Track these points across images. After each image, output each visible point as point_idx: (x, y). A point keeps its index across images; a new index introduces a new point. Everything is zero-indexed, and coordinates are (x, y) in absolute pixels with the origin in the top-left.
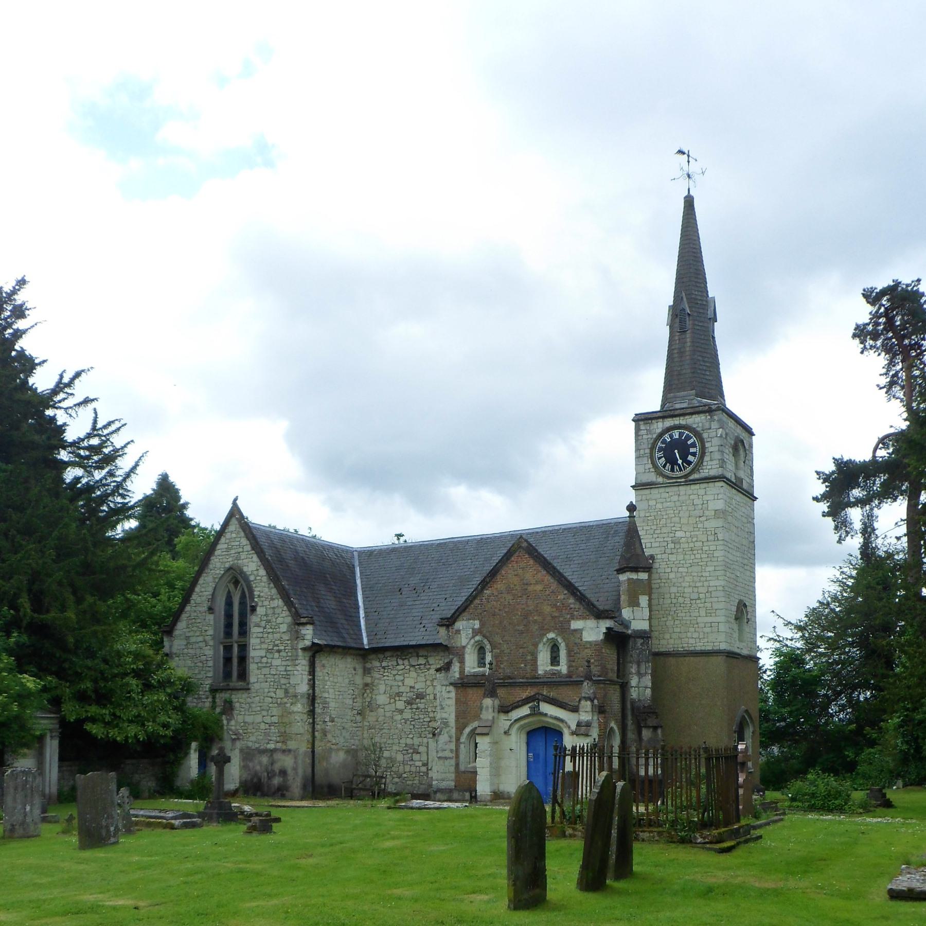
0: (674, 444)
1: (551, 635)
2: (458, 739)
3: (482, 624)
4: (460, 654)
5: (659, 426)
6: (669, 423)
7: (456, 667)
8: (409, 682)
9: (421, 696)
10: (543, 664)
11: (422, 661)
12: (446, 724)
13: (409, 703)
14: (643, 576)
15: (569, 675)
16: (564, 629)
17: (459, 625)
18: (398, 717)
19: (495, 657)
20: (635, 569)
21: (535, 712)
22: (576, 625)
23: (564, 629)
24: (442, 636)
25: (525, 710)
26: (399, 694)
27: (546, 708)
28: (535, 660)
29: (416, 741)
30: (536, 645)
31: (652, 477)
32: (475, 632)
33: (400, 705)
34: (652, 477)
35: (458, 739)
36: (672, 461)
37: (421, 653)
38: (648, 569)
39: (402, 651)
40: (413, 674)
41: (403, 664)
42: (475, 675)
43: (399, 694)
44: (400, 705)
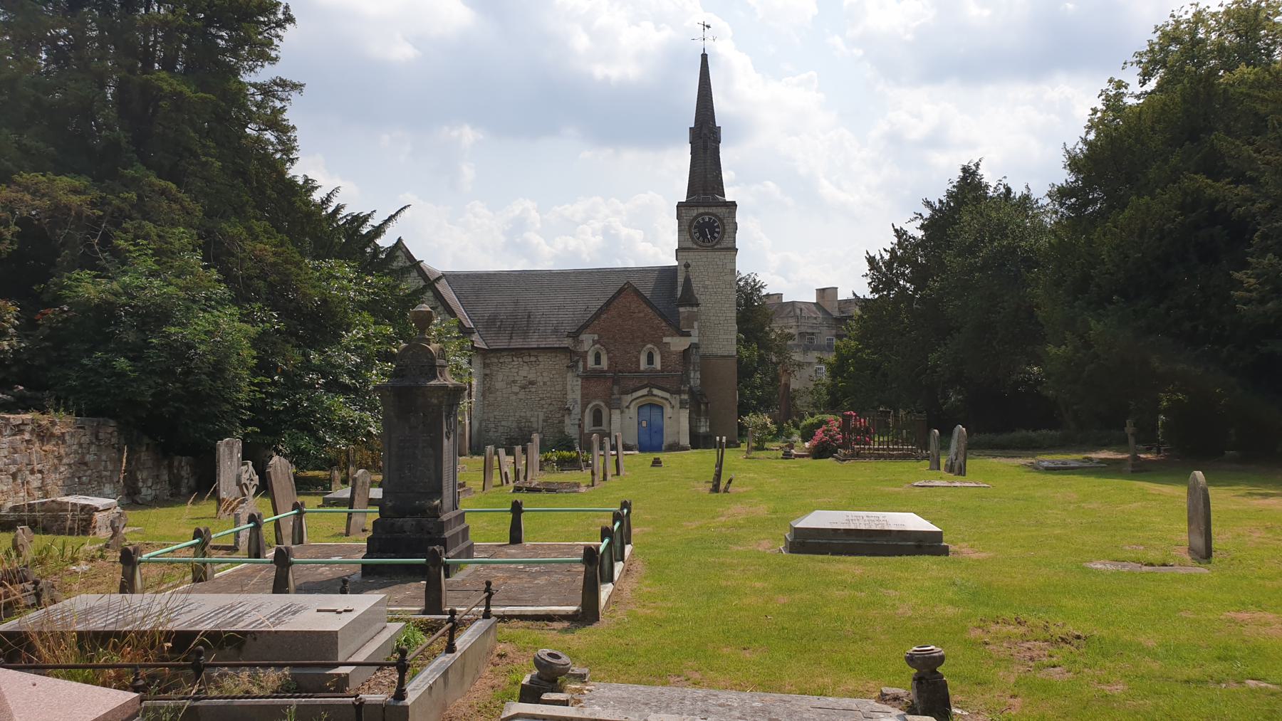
0: (706, 225)
1: (649, 346)
2: (583, 412)
3: (600, 337)
4: (584, 356)
5: (695, 212)
6: (701, 210)
7: (581, 364)
8: (523, 373)
9: (532, 383)
10: (643, 365)
11: (533, 359)
12: (576, 402)
13: (523, 387)
14: (695, 309)
15: (662, 371)
16: (659, 343)
17: (583, 337)
18: (514, 397)
19: (609, 359)
20: (692, 305)
21: (650, 394)
22: (666, 340)
23: (659, 343)
24: (567, 343)
25: (645, 392)
26: (514, 382)
27: (656, 391)
28: (638, 361)
29: (529, 414)
30: (639, 352)
31: (690, 244)
32: (595, 342)
33: (516, 389)
34: (690, 244)
35: (583, 412)
36: (703, 235)
37: (533, 353)
38: (698, 305)
39: (517, 352)
40: (526, 368)
41: (517, 361)
42: (594, 370)
43: (514, 382)
44: (516, 389)
